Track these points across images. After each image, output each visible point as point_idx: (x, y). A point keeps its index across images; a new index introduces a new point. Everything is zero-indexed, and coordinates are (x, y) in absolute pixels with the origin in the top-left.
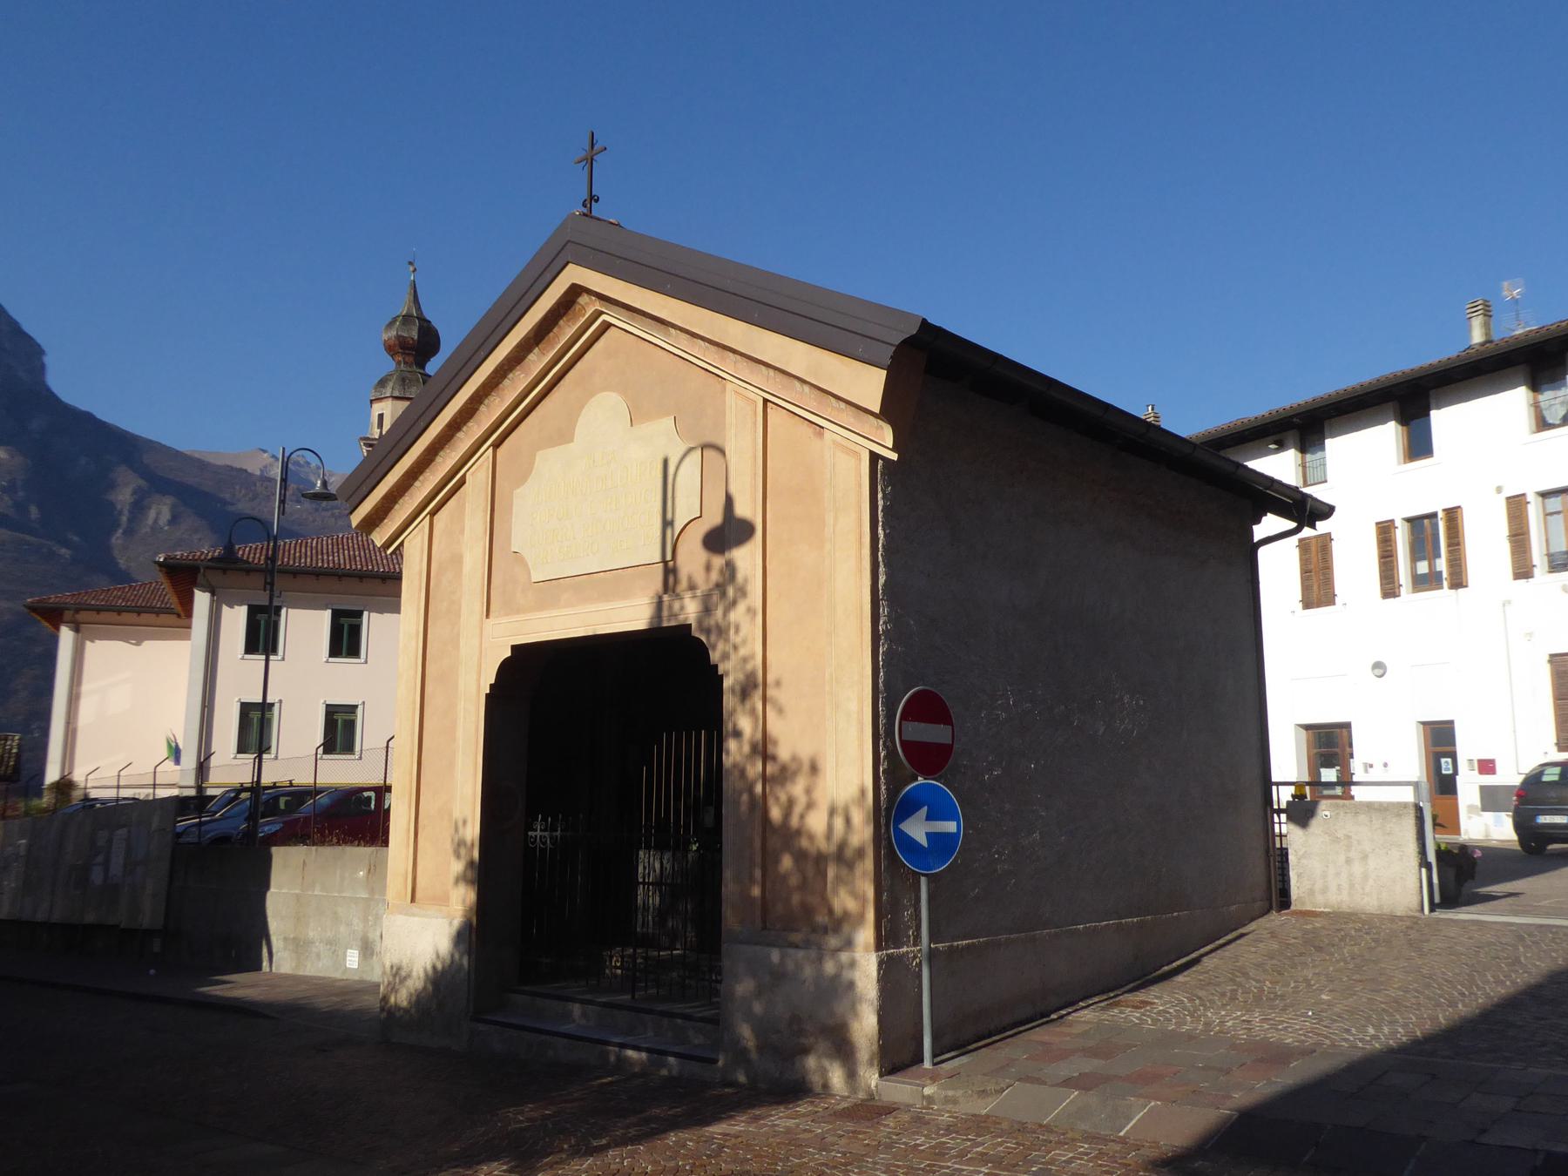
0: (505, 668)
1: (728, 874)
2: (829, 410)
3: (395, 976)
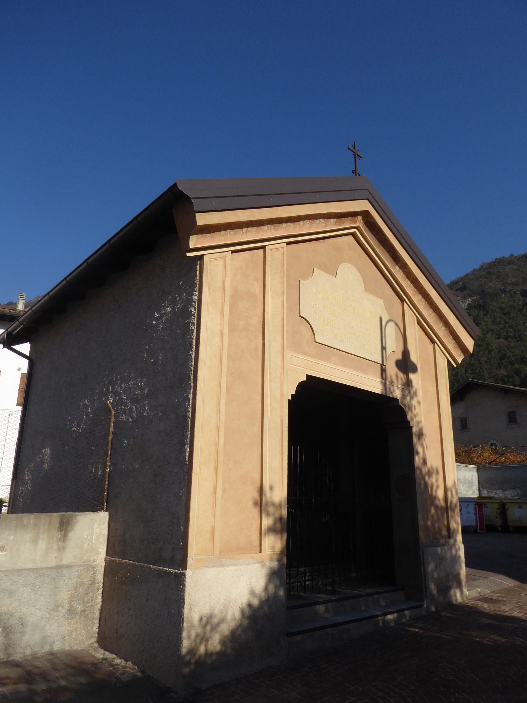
0: (301, 387)
1: (420, 517)
2: (446, 340)
3: (204, 627)
